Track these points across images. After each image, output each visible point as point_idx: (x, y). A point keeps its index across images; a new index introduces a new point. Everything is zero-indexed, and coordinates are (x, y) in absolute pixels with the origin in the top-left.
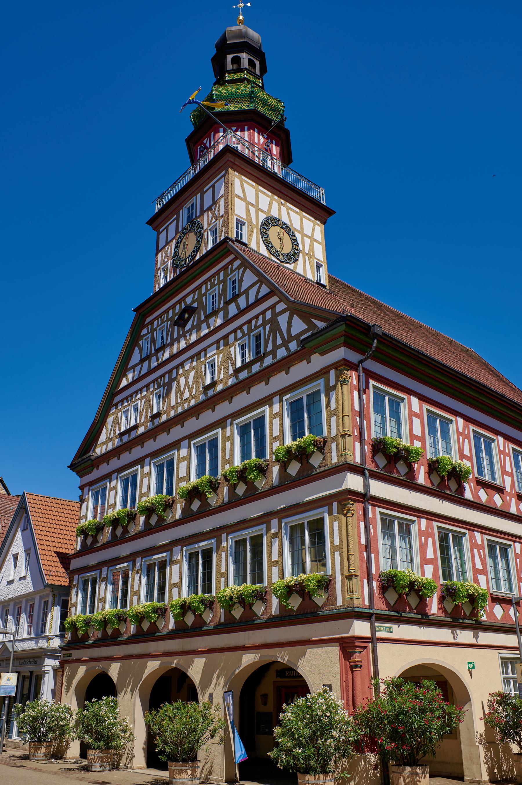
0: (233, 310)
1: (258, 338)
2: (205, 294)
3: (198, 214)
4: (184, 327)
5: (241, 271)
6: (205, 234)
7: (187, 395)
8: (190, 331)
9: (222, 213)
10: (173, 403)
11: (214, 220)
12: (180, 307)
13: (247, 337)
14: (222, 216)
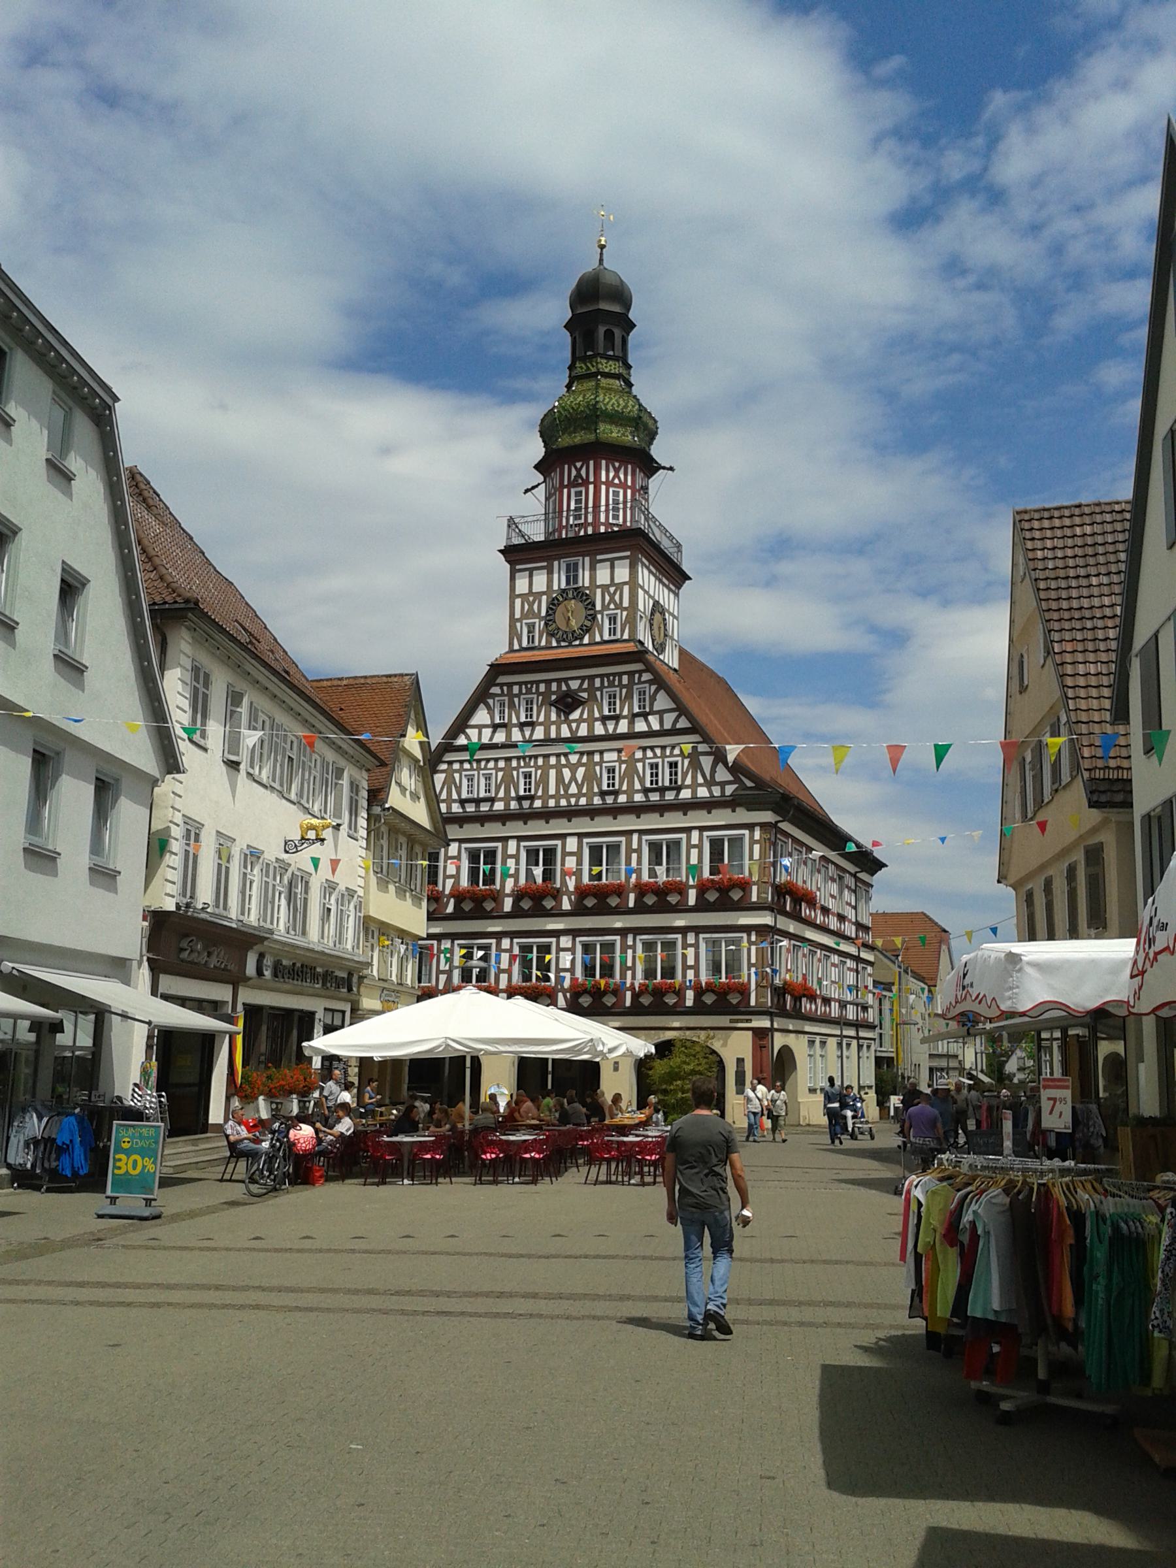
0: (640, 726)
1: (673, 765)
2: (601, 689)
3: (587, 584)
4: (567, 714)
5: (653, 688)
6: (599, 616)
7: (573, 789)
8: (580, 721)
9: (626, 604)
10: (552, 791)
11: (612, 606)
12: (559, 687)
13: (660, 760)
14: (626, 609)
